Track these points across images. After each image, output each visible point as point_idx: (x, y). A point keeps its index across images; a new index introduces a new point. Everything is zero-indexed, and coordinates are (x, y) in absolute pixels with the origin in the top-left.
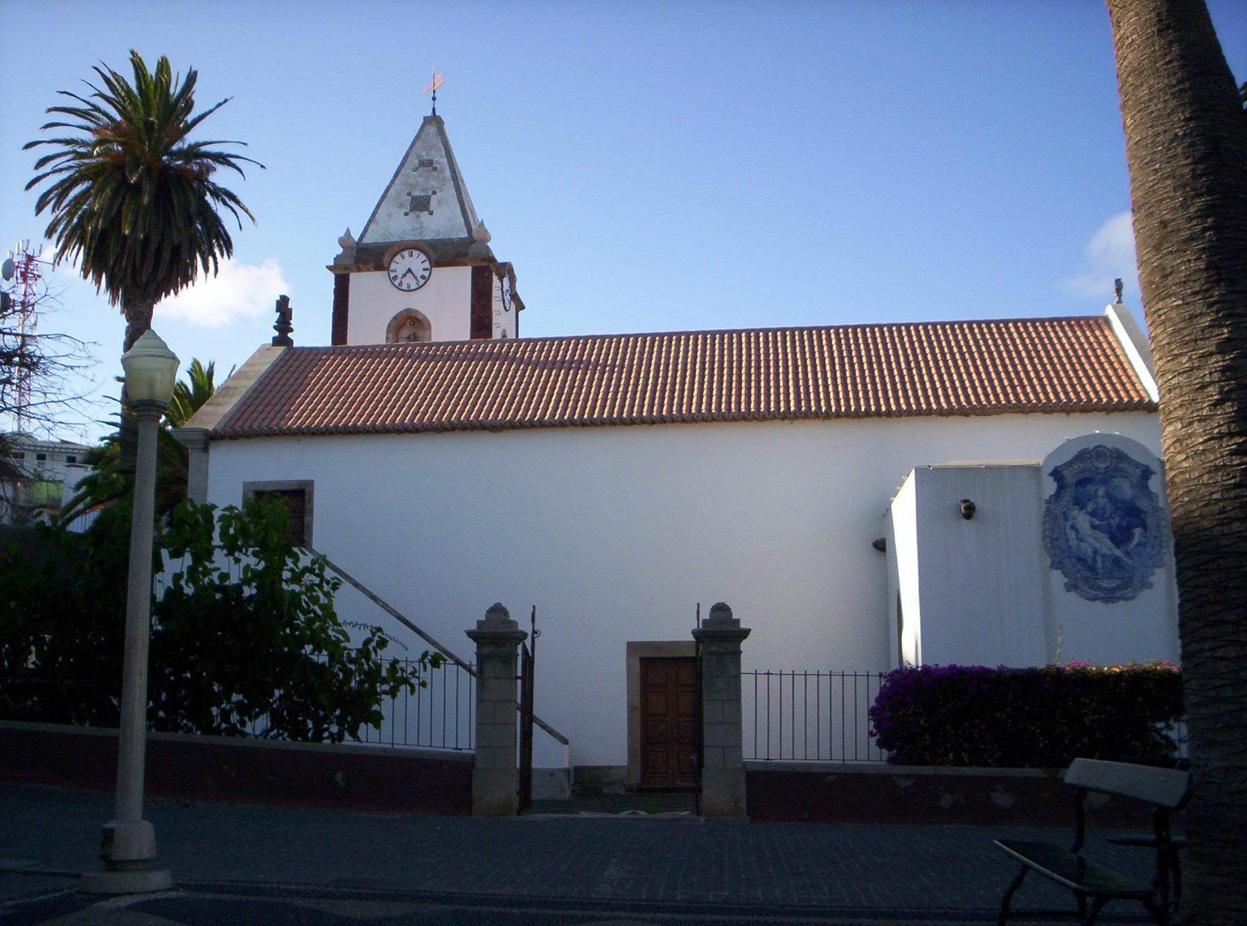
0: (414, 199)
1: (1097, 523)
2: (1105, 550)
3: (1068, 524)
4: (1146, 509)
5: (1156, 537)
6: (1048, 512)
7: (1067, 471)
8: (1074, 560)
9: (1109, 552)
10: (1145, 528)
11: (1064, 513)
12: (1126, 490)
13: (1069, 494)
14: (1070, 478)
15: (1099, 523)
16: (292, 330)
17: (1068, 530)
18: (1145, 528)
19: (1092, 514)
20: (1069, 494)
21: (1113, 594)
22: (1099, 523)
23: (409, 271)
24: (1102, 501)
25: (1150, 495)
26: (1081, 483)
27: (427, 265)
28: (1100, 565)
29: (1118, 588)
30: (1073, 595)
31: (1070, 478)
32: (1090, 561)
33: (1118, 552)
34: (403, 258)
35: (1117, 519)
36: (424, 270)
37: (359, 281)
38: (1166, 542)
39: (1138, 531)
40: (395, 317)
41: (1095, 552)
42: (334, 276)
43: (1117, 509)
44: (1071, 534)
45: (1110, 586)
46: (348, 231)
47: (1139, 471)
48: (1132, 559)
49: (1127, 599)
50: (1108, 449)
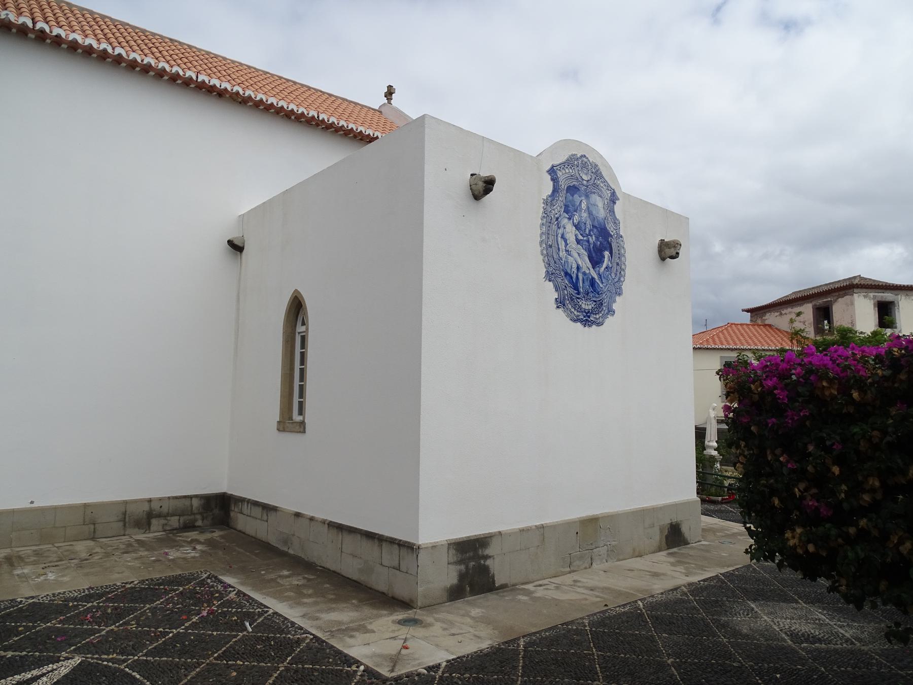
1: (580, 237)
2: (584, 269)
3: (560, 231)
4: (612, 234)
7: (561, 174)
8: (563, 273)
9: (587, 272)
10: (611, 253)
13: (561, 198)
17: (559, 239)
18: (611, 253)
20: (561, 198)
21: (589, 317)
25: (616, 222)
26: (572, 190)
28: (581, 286)
30: (560, 311)
32: (574, 276)
39: (607, 254)
41: (578, 268)
45: (587, 307)
48: (602, 283)
50: (589, 160)
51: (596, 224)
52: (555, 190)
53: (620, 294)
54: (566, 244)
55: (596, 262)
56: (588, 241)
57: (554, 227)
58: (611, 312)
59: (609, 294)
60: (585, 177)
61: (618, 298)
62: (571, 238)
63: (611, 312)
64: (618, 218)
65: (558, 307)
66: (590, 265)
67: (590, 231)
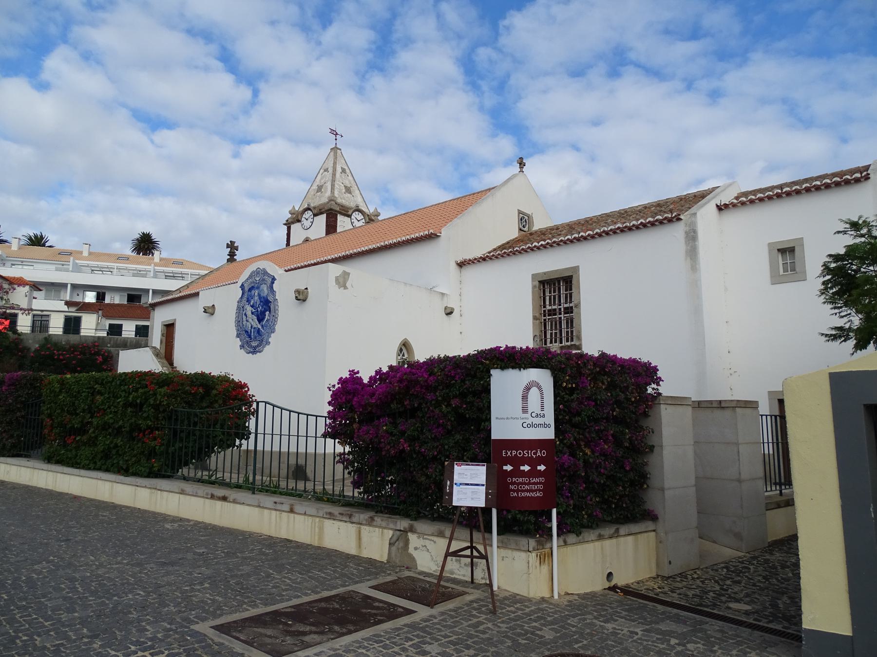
1: (254, 310)
2: (255, 326)
3: (244, 312)
5: (273, 316)
6: (238, 308)
13: (246, 296)
14: (247, 289)
16: (236, 255)
19: (252, 306)
20: (246, 296)
24: (256, 298)
26: (250, 290)
29: (258, 346)
31: (247, 289)
32: (249, 331)
33: (260, 327)
37: (294, 227)
39: (267, 313)
41: (251, 327)
43: (261, 302)
44: (244, 317)
47: (270, 279)
48: (264, 329)
51: (262, 300)
52: (243, 294)
53: (274, 332)
54: (247, 317)
55: (260, 320)
56: (257, 311)
57: (241, 311)
58: (268, 343)
59: (267, 334)
60: (258, 279)
61: (272, 335)
62: (249, 313)
63: (268, 343)
66: (258, 325)
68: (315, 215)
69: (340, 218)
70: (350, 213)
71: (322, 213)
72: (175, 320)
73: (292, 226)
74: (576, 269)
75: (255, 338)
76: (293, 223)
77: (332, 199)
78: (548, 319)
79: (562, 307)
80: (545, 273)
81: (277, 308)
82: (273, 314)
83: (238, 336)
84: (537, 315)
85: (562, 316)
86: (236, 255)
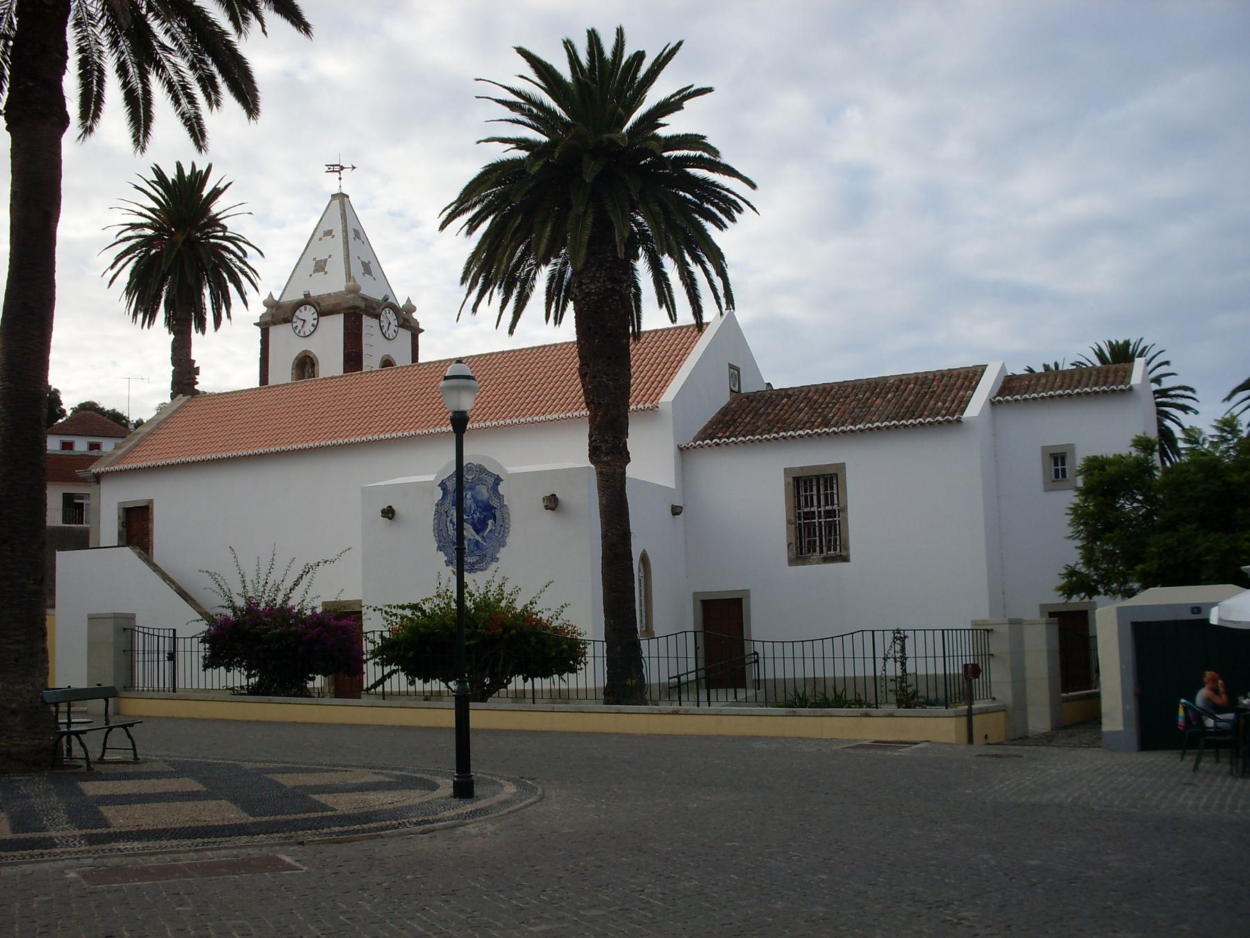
0: (317, 262)
3: (449, 519)
5: (502, 526)
6: (437, 513)
9: (472, 538)
11: (446, 512)
12: (484, 492)
15: (467, 517)
16: (197, 383)
17: (448, 523)
22: (467, 517)
23: (304, 321)
25: (500, 497)
27: (315, 316)
29: (477, 563)
33: (479, 539)
34: (301, 312)
35: (478, 514)
36: (314, 319)
37: (274, 331)
38: (507, 528)
39: (490, 522)
40: (296, 358)
42: (260, 330)
45: (472, 561)
46: (271, 295)
48: (486, 542)
49: (482, 570)
51: (480, 504)
53: (503, 546)
56: (473, 518)
57: (444, 517)
61: (502, 550)
64: (501, 493)
65: (447, 565)
66: (475, 535)
67: (474, 511)
68: (322, 313)
69: (367, 322)
70: (378, 311)
71: (337, 312)
72: (151, 501)
73: (272, 330)
74: (842, 466)
75: (473, 552)
76: (275, 324)
77: (354, 290)
78: (805, 524)
79: (822, 509)
80: (802, 468)
81: (506, 515)
82: (499, 522)
83: (440, 549)
84: (793, 518)
85: (822, 520)
86: (197, 383)
